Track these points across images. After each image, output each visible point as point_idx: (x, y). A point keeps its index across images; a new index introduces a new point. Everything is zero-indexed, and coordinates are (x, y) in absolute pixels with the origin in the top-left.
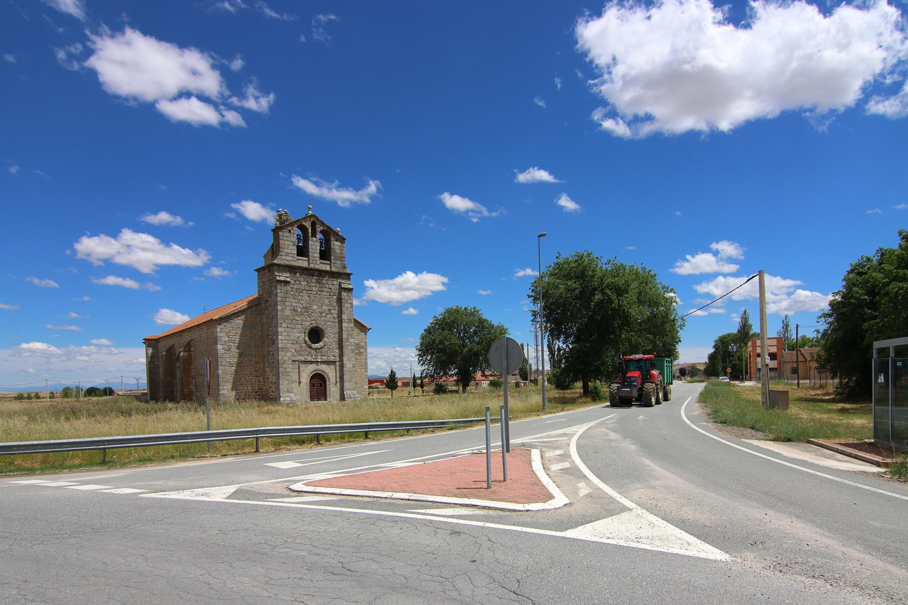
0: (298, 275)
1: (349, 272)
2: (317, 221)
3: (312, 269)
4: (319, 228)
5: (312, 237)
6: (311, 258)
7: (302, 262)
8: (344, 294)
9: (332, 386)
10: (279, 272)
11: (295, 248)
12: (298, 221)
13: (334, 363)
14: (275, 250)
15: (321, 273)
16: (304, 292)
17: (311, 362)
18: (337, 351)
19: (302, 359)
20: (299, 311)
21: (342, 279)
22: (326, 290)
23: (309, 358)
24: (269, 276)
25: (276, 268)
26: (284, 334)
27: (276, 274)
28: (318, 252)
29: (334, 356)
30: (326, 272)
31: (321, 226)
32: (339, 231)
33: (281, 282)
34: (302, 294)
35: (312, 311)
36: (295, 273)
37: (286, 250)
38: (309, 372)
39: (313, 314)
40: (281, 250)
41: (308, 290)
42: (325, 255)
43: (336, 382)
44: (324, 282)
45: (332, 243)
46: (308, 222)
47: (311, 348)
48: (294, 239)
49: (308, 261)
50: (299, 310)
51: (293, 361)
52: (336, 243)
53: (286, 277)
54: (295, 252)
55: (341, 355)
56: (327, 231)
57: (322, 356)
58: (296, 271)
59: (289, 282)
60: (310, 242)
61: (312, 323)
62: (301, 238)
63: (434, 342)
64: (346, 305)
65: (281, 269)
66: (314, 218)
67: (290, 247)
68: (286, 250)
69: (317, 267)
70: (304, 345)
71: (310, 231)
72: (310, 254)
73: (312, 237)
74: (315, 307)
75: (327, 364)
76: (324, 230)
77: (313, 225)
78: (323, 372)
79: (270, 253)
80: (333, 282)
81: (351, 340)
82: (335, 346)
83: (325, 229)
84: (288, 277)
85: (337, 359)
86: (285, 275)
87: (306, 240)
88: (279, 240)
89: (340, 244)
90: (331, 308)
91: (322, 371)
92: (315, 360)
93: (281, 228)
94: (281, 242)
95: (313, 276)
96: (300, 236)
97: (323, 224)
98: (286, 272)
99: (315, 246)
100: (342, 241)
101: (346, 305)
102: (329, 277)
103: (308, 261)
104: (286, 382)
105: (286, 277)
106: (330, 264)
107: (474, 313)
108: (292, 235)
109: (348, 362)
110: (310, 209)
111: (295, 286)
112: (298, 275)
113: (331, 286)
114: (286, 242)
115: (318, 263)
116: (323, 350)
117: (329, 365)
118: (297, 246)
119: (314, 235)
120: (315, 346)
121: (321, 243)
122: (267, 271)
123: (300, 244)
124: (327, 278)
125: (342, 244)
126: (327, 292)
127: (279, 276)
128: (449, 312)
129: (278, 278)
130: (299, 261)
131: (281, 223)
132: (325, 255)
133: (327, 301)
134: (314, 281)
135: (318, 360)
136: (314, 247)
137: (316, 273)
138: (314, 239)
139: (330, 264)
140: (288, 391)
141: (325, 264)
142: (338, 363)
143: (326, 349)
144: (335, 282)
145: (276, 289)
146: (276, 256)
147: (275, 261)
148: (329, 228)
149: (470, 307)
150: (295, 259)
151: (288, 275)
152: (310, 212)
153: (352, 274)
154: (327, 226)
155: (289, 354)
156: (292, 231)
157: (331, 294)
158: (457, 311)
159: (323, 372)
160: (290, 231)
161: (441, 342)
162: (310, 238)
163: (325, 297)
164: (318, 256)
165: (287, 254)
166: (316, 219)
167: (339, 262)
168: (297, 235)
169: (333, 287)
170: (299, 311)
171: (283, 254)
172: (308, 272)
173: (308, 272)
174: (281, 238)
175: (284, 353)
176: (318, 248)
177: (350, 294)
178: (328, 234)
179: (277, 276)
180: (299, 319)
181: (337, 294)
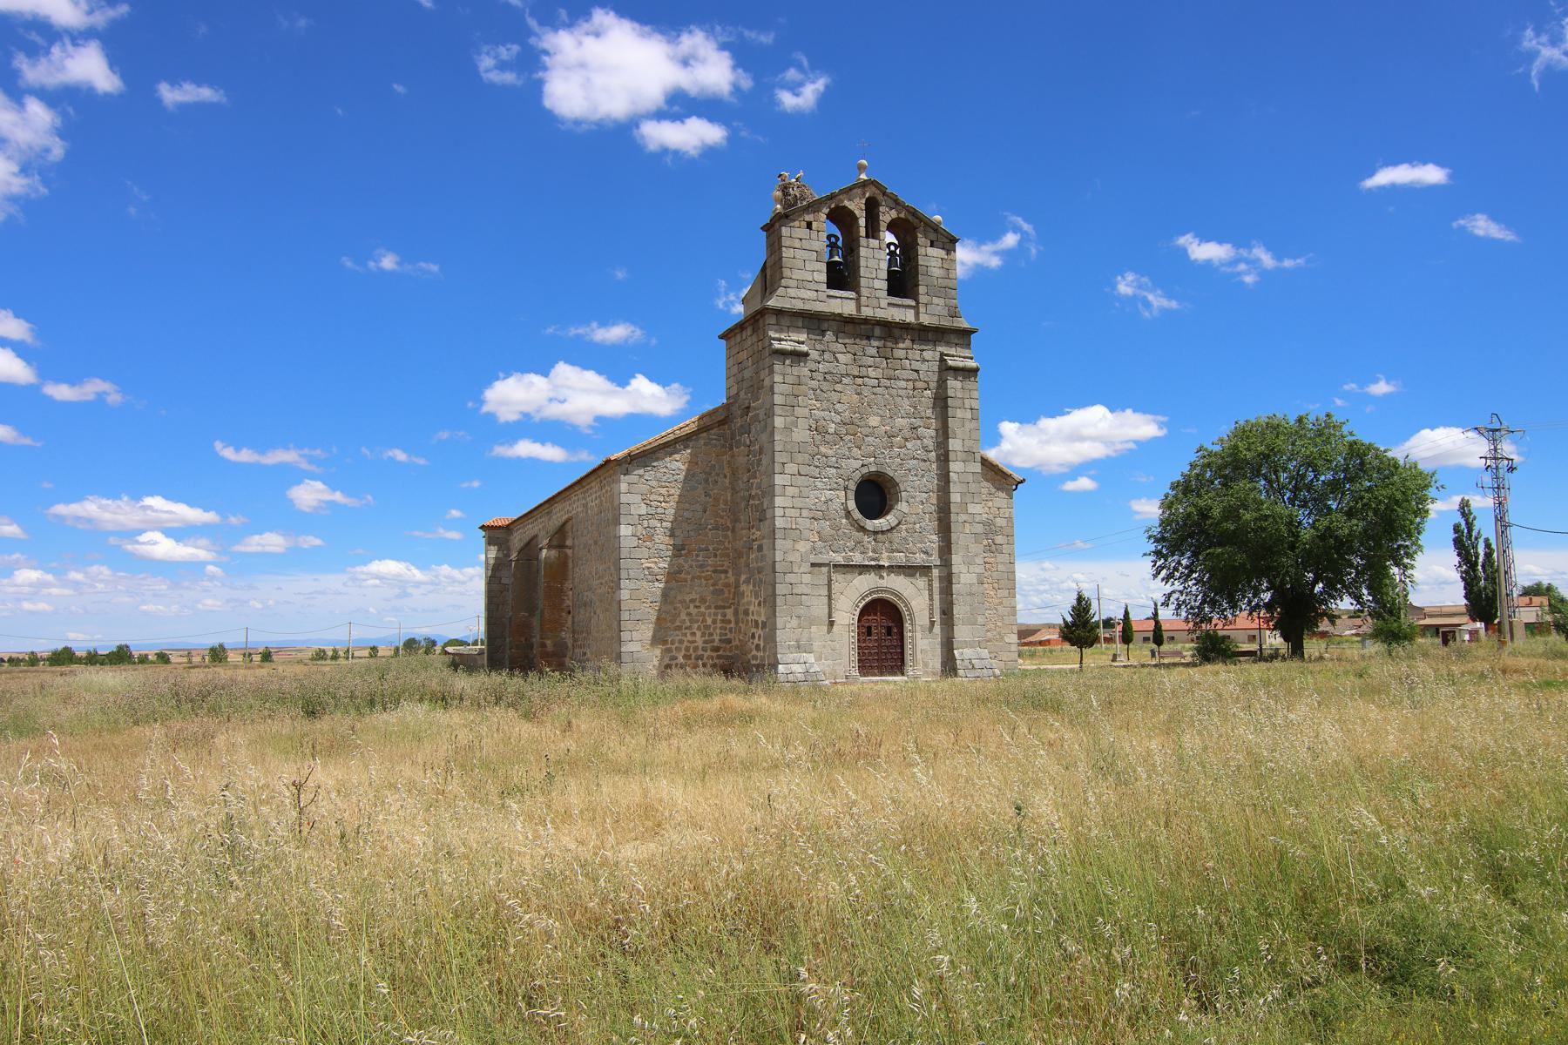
0: (829, 336)
1: (966, 325)
2: (880, 198)
3: (866, 321)
4: (887, 215)
5: (867, 236)
6: (864, 291)
7: (842, 304)
8: (954, 384)
9: (919, 635)
10: (781, 331)
11: (824, 267)
12: (832, 197)
13: (925, 570)
14: (770, 277)
15: (891, 331)
16: (845, 380)
17: (863, 569)
18: (935, 538)
19: (839, 558)
20: (831, 431)
21: (948, 344)
23: (858, 559)
24: (753, 344)
25: (772, 319)
26: (790, 491)
27: (772, 334)
28: (884, 275)
29: (926, 553)
30: (905, 327)
31: (891, 209)
32: (940, 223)
33: (783, 354)
34: (839, 387)
35: (866, 431)
36: (823, 333)
37: (797, 275)
38: (855, 596)
39: (870, 439)
40: (786, 272)
41: (855, 377)
42: (902, 282)
44: (900, 353)
45: (921, 251)
46: (857, 200)
47: (862, 529)
48: (821, 244)
49: (858, 300)
50: (832, 428)
51: (813, 565)
52: (931, 251)
53: (798, 342)
54: (823, 277)
55: (946, 549)
56: (906, 220)
57: (893, 551)
58: (825, 326)
59: (806, 355)
60: (863, 252)
61: (865, 462)
62: (840, 243)
63: (1204, 514)
64: (959, 413)
65: (785, 321)
66: (874, 189)
67: (809, 266)
68: (797, 275)
69: (881, 314)
70: (844, 521)
71: (862, 222)
72: (863, 282)
73: (867, 236)
74: (874, 421)
76: (899, 218)
77: (872, 207)
79: (759, 286)
80: (924, 353)
81: (972, 508)
82: (930, 523)
83: (902, 215)
84: (803, 343)
85: (935, 559)
86: (795, 337)
87: (851, 249)
88: (780, 247)
89: (942, 253)
90: (917, 422)
91: (893, 594)
92: (873, 563)
93: (786, 216)
94: (786, 253)
95: (868, 338)
96: (837, 239)
97: (896, 203)
98: (797, 329)
99: (875, 258)
100: (947, 246)
102: (913, 341)
103: (858, 300)
105: (798, 342)
106: (916, 308)
107: (1325, 431)
108: (814, 234)
109: (963, 569)
110: (861, 168)
111: (821, 366)
112: (829, 336)
113: (916, 365)
114: (799, 253)
115: (884, 303)
116: (895, 534)
117: (912, 575)
118: (827, 263)
119: (873, 231)
120: (870, 524)
121: (892, 254)
122: (749, 331)
123: (836, 259)
124: (908, 343)
125: (948, 253)
126: (907, 380)
127: (780, 340)
128: (1243, 433)
129: (776, 345)
130: (833, 300)
131: (787, 205)
132: (902, 282)
133: (906, 405)
134: (873, 351)
135: (881, 563)
136: (872, 263)
137: (877, 331)
138: (874, 243)
139: (916, 308)
141: (903, 306)
142: (936, 572)
143: (904, 534)
144: (928, 355)
145: (772, 372)
146: (773, 292)
147: (772, 303)
148: (914, 213)
149: (1314, 411)
150: (822, 296)
151: (803, 337)
152: (861, 177)
153: (973, 331)
154: (907, 209)
155: (803, 547)
156: (814, 225)
157: (919, 385)
158: (1274, 428)
160: (809, 226)
161: (1231, 513)
162: (863, 241)
163: (902, 393)
164: (884, 285)
165: (801, 284)
166: (877, 192)
167: (941, 301)
168: (829, 237)
169: (924, 367)
170: (831, 431)
171: (792, 283)
172: (856, 328)
173: (856, 328)
174: (785, 242)
175: (788, 544)
176: (884, 266)
177: (969, 384)
178: (909, 228)
179: (774, 339)
180: (830, 452)
181: (933, 385)
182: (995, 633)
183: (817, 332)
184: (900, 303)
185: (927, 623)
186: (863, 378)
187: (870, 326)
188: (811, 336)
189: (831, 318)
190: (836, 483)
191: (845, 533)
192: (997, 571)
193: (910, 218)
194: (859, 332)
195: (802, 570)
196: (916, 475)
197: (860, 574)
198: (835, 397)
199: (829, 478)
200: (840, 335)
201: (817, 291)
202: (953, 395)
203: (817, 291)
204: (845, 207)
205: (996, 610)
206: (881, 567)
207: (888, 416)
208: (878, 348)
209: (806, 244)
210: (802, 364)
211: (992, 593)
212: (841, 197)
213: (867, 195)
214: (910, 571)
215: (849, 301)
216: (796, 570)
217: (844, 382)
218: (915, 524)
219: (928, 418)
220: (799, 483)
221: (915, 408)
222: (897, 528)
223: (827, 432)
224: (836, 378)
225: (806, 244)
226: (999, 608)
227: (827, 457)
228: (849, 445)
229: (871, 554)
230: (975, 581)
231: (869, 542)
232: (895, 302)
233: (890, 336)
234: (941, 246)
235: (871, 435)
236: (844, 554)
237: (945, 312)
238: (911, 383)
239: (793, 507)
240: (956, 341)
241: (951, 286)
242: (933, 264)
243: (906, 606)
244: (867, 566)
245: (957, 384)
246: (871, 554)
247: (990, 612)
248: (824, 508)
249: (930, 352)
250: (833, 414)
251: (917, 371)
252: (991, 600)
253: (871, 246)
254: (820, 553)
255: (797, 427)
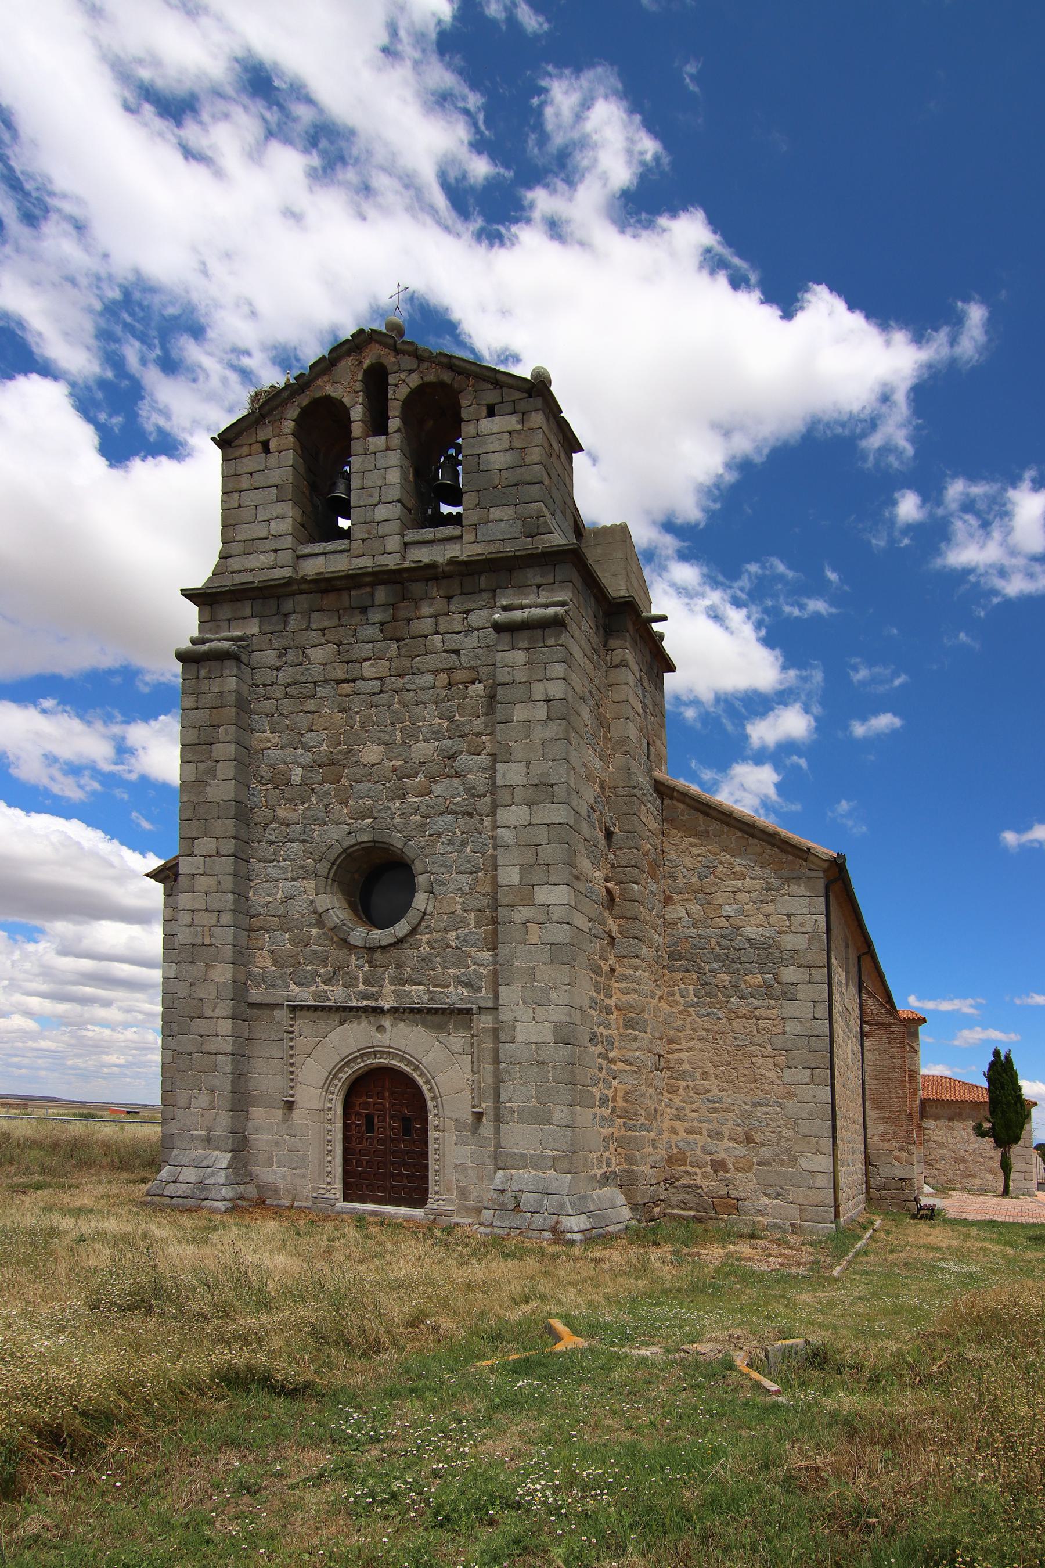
9: (450, 1136)
13: (462, 1015)
16: (321, 691)
17: (346, 1013)
19: (305, 995)
20: (296, 779)
22: (431, 662)
23: (337, 994)
26: (203, 883)
29: (467, 985)
30: (428, 573)
34: (311, 705)
35: (358, 772)
38: (333, 1061)
39: (365, 786)
41: (339, 682)
43: (479, 1116)
44: (425, 626)
47: (345, 943)
50: (297, 774)
57: (406, 982)
61: (354, 827)
64: (520, 713)
70: (314, 931)
74: (371, 753)
75: (425, 1025)
78: (409, 1063)
80: (472, 616)
81: (542, 895)
90: (458, 744)
101: (520, 713)
104: (204, 1099)
109: (524, 1013)
111: (281, 673)
113: (455, 641)
115: (393, 543)
116: (407, 951)
117: (440, 1028)
124: (440, 604)
126: (436, 672)
133: (432, 718)
134: (372, 632)
135: (381, 1003)
140: (208, 1140)
143: (424, 949)
159: (409, 1063)
163: (425, 696)
167: (507, 513)
169: (472, 641)
170: (296, 779)
180: (292, 816)
182: (777, 1149)
183: (275, 619)
184: (431, 536)
185: (468, 1116)
186: (354, 681)
187: (368, 589)
188: (267, 628)
189: (295, 587)
190: (302, 867)
191: (315, 952)
192: (784, 1033)
193: (446, 377)
194: (347, 605)
195: (219, 1012)
196: (450, 843)
197: (342, 1023)
198: (303, 720)
199: (290, 860)
200: (315, 616)
201: (275, 551)
202: (507, 679)
203: (275, 551)
204: (328, 398)
205: (780, 1105)
206: (379, 1011)
207: (399, 740)
208: (382, 624)
209: (259, 480)
210: (227, 672)
211: (770, 1074)
212: (320, 382)
213: (366, 363)
214: (437, 1019)
215: (337, 556)
216: (208, 1013)
217: (319, 695)
218: (446, 931)
219: (478, 735)
220: (217, 869)
221: (451, 720)
222: (411, 940)
223: (288, 784)
224: (304, 691)
225: (259, 480)
226: (789, 1103)
227: (288, 825)
228: (326, 801)
229: (362, 987)
230: (550, 1038)
231: (358, 967)
232: (419, 538)
233: (404, 600)
234: (509, 408)
235: (367, 778)
236: (314, 988)
237: (517, 530)
238: (443, 677)
239: (207, 910)
240: (539, 580)
241: (528, 478)
242: (491, 448)
243: (427, 1082)
244: (351, 1008)
245: (520, 657)
246: (362, 987)
247: (765, 1109)
248: (281, 910)
249: (484, 613)
250: (300, 751)
251: (456, 652)
252: (768, 1087)
253: (372, 448)
254: (274, 986)
255: (214, 777)
